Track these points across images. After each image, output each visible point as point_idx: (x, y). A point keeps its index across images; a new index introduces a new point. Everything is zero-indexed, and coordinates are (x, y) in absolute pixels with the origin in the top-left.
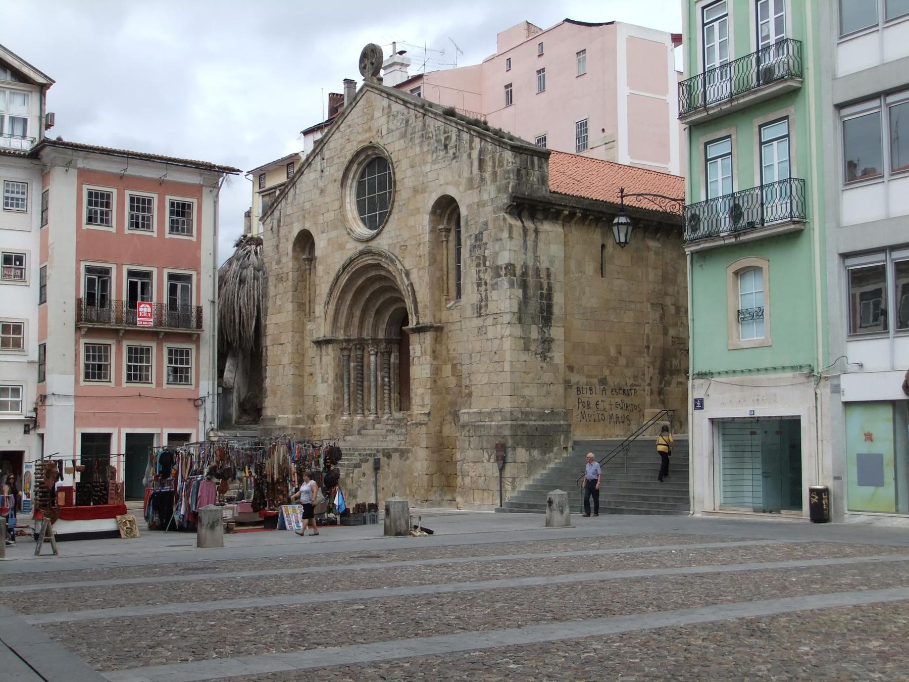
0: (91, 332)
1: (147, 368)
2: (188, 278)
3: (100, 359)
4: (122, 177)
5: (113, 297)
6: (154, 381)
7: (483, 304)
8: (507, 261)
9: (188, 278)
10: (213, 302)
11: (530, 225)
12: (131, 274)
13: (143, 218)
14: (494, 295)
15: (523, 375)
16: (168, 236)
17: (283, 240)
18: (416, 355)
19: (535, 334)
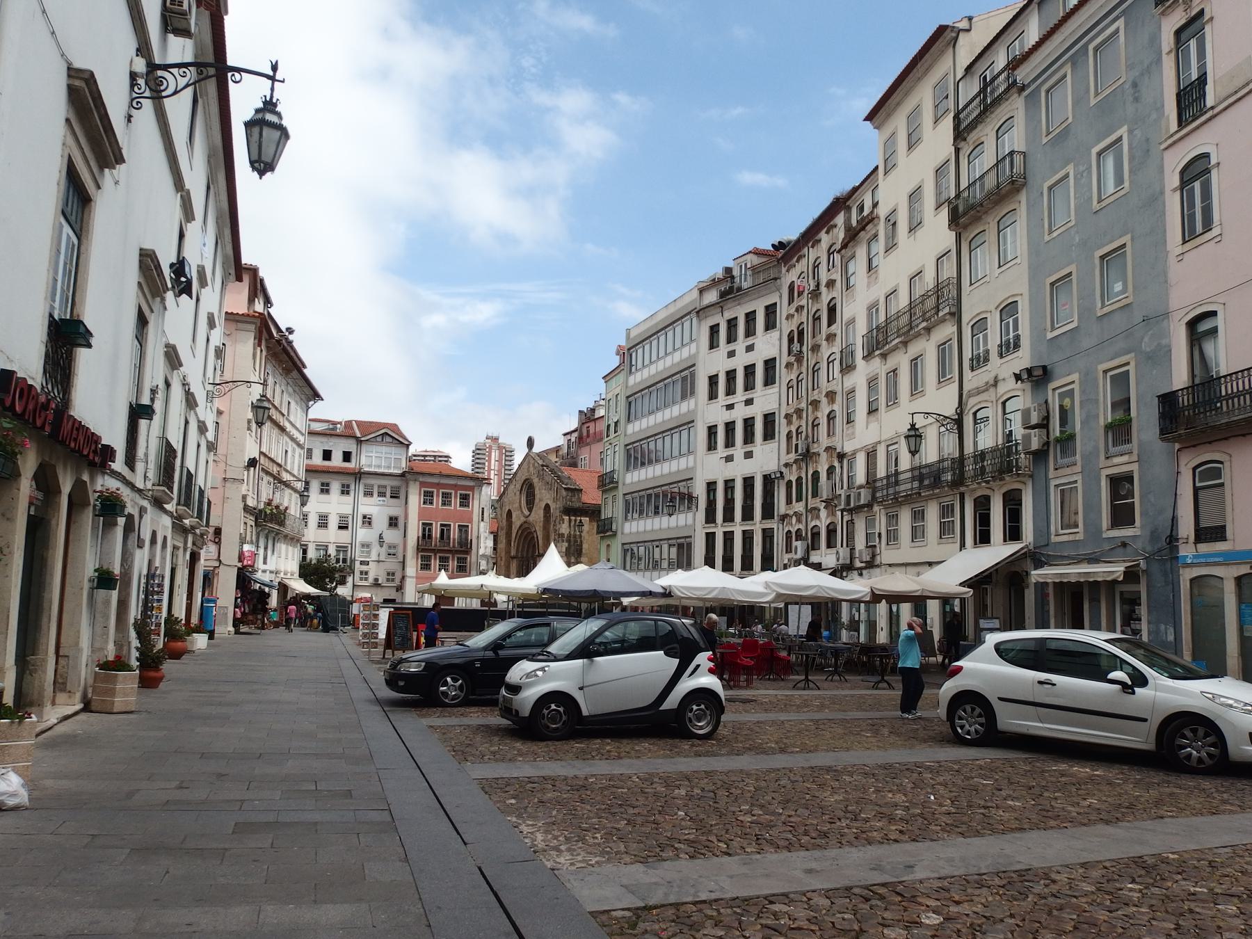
0: (423, 550)
4: (438, 484)
11: (573, 518)
12: (442, 525)
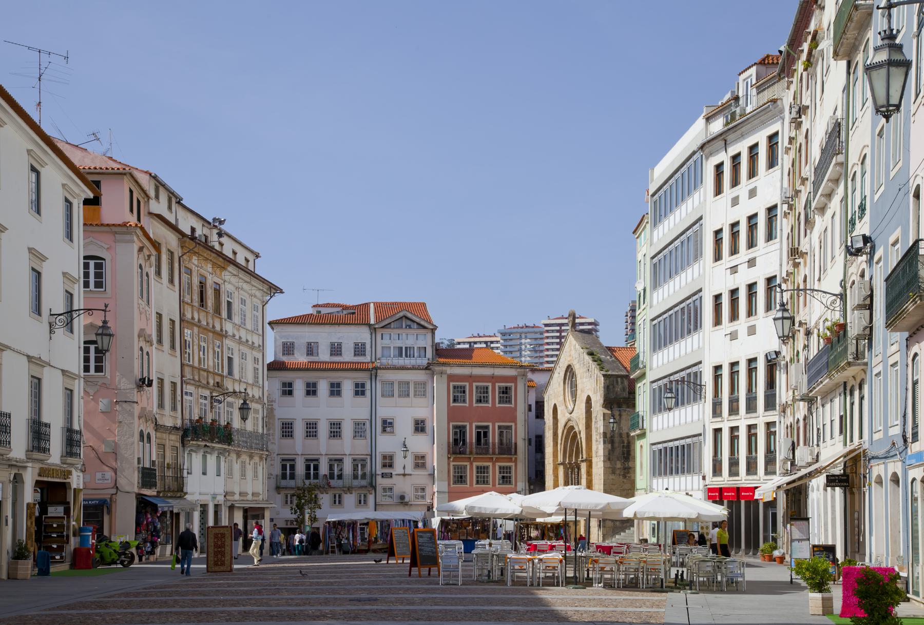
1: (487, 476)
3: (461, 473)
6: (491, 483)
9: (509, 428)
10: (525, 439)
13: (484, 397)
16: (497, 405)
19: (619, 465)
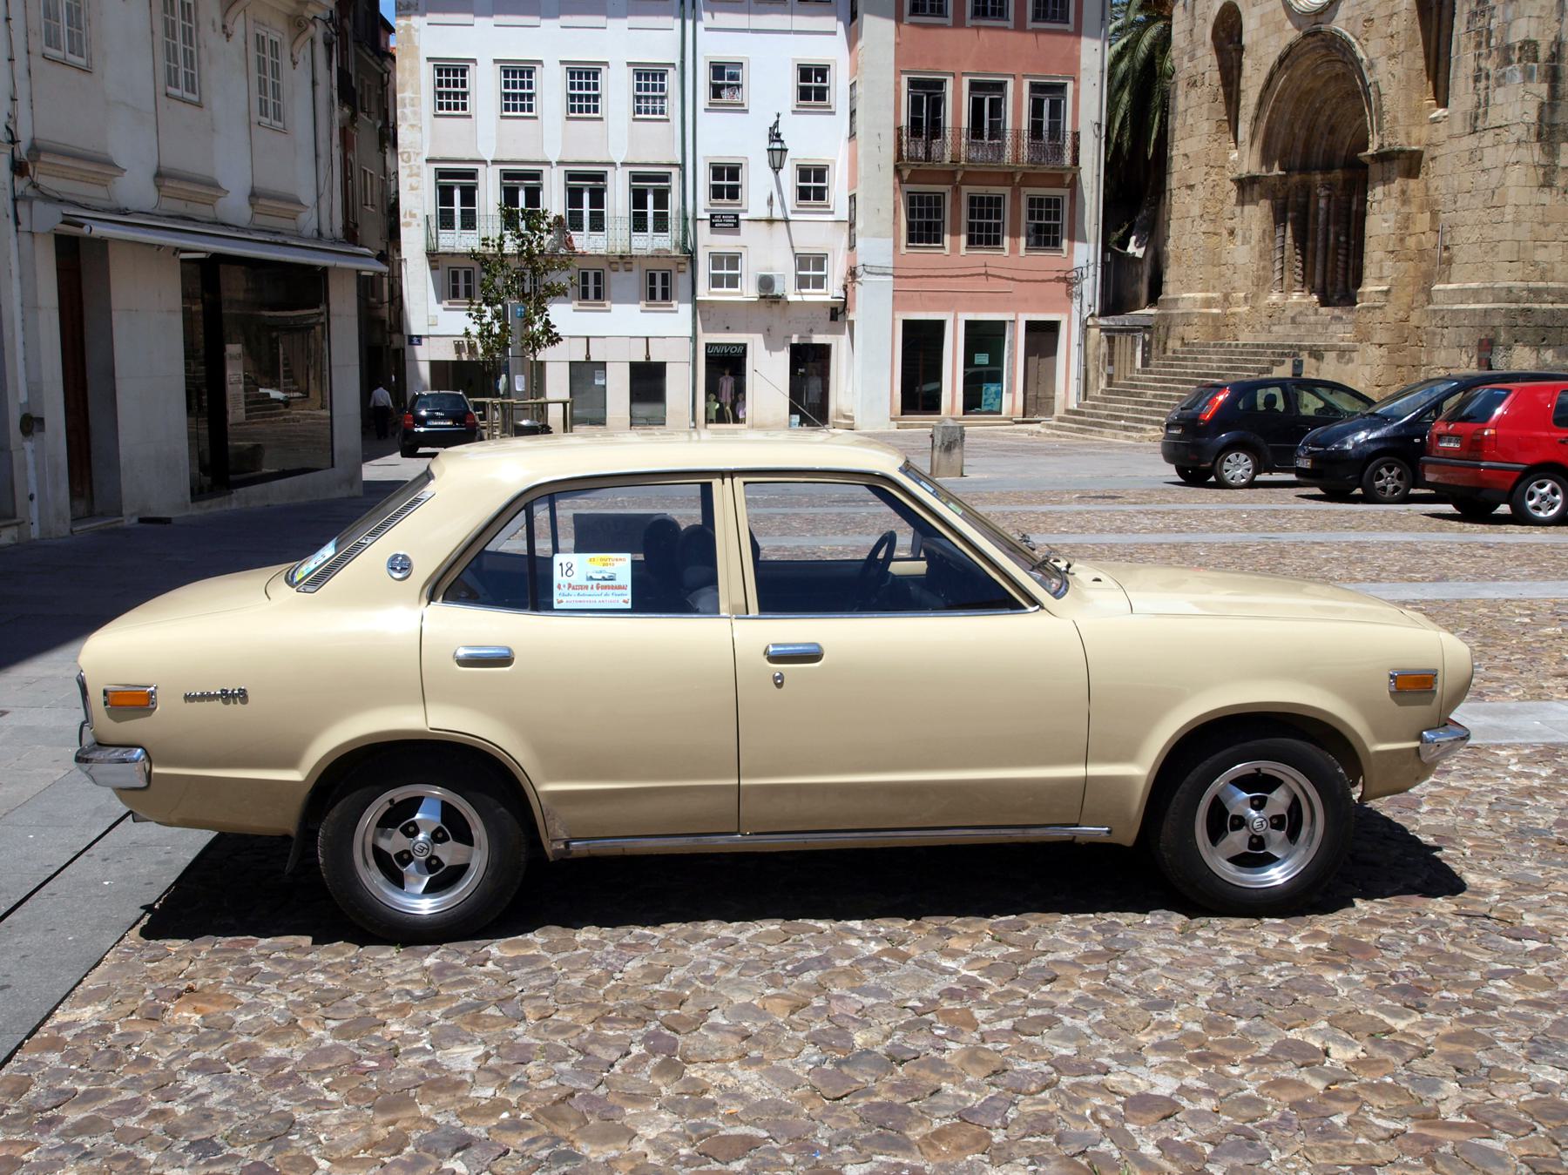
2: (1062, 88)
3: (929, 215)
5: (949, 123)
7: (1481, 110)
8: (1522, 38)
10: (1100, 126)
14: (1499, 95)
15: (1536, 227)
17: (1199, 22)
18: (1376, 198)
